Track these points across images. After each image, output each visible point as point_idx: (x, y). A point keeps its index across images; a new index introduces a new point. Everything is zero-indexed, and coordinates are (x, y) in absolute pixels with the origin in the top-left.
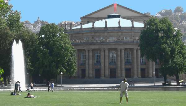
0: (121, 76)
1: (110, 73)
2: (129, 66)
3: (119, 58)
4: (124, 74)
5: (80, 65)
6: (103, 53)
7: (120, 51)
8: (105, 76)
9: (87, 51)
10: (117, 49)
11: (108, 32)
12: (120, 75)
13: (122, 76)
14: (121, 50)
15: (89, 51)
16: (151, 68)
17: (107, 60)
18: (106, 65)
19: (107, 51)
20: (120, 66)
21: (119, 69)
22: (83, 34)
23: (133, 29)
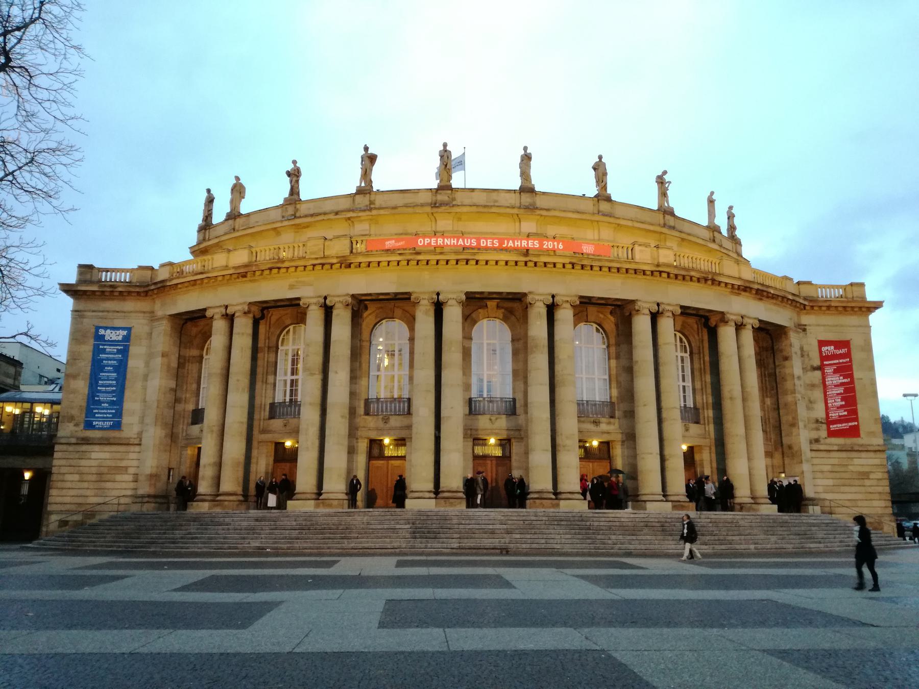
0: (556, 493)
2: (604, 427)
3: (539, 361)
7: (544, 311)
8: (437, 490)
12: (549, 487)
13: (562, 487)
14: (551, 309)
16: (742, 446)
17: (451, 376)
19: (453, 315)
21: (540, 439)
23: (604, 206)
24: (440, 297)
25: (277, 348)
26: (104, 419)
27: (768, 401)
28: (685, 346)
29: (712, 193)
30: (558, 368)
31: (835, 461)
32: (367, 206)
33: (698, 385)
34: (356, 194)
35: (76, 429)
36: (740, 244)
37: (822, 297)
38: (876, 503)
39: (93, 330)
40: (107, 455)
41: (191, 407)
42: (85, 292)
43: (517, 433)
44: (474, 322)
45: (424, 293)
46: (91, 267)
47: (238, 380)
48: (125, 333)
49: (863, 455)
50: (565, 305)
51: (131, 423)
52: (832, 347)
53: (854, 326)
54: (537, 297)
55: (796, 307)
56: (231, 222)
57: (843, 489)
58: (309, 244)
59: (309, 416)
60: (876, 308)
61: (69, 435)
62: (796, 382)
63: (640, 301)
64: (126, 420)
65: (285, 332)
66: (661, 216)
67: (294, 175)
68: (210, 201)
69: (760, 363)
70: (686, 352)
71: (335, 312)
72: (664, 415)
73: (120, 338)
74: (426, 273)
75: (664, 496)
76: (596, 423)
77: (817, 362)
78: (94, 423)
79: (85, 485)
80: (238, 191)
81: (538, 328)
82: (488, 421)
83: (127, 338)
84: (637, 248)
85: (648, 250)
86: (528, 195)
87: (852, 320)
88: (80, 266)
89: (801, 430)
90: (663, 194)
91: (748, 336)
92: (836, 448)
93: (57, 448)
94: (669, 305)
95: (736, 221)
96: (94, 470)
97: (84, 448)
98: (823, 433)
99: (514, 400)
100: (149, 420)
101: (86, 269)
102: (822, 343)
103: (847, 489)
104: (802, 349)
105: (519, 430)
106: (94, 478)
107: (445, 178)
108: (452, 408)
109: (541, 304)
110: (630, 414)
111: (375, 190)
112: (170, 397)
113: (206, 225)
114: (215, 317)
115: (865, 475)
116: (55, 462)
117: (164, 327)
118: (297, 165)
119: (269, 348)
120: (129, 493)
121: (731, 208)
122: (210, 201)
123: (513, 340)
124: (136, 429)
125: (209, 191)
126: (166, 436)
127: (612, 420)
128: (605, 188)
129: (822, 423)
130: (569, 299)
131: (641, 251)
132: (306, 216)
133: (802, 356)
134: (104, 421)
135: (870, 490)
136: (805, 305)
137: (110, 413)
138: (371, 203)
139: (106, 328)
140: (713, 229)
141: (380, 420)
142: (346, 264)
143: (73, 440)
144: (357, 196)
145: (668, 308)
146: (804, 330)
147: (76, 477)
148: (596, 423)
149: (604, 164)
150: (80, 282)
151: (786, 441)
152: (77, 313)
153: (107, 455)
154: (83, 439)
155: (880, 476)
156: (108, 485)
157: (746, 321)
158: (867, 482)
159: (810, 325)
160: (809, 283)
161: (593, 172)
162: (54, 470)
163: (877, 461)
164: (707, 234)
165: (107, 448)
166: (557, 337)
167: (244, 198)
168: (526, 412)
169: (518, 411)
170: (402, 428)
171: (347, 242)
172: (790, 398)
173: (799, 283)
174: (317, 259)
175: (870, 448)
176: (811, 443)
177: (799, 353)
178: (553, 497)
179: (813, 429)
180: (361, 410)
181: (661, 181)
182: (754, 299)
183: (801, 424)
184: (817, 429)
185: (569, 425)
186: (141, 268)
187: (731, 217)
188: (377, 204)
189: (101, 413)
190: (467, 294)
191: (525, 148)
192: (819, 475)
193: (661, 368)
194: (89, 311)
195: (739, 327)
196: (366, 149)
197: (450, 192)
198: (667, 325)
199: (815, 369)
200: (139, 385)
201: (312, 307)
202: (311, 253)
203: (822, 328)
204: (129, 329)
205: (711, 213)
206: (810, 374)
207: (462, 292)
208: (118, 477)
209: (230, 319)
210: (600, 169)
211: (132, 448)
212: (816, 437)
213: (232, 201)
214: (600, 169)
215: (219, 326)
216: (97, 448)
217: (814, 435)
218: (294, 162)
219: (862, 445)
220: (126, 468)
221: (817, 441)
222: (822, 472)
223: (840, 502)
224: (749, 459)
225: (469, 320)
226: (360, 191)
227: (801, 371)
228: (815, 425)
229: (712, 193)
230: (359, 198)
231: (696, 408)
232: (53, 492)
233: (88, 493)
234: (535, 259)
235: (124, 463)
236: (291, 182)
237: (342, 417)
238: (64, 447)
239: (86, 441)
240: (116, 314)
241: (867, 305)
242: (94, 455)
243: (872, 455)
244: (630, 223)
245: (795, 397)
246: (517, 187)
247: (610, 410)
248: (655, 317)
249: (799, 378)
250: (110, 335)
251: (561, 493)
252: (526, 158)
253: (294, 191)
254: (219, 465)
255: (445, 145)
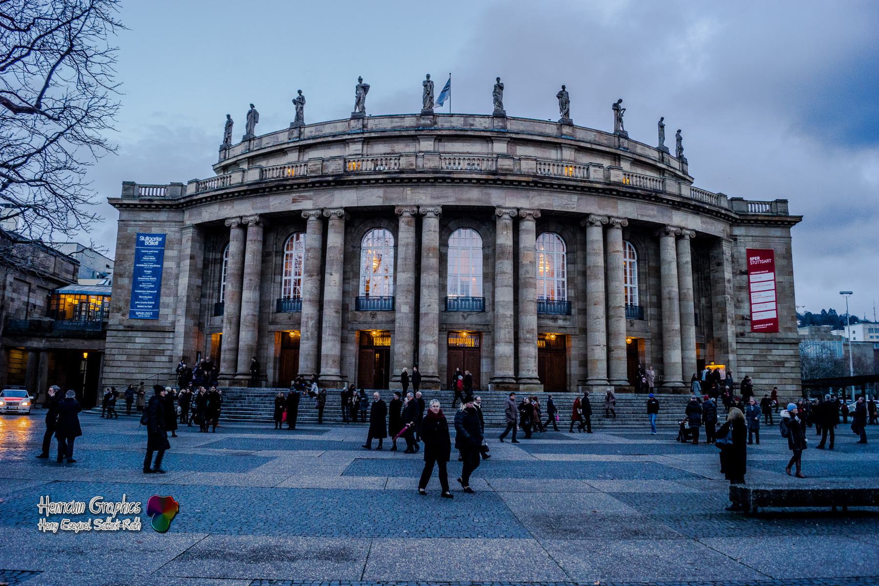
1: (445, 362)
2: (560, 322)
3: (506, 266)
4: (531, 367)
5: (273, 308)
6: (406, 234)
7: (509, 222)
9: (313, 224)
10: (493, 209)
11: (439, 138)
12: (511, 373)
13: (523, 373)
15: (324, 221)
16: (678, 339)
17: (429, 278)
18: (423, 310)
19: (432, 224)
20: (510, 312)
21: (505, 332)
22: (303, 149)
23: (566, 130)
24: (421, 210)
25: (283, 253)
26: (145, 310)
27: (703, 301)
28: (633, 253)
29: (662, 119)
30: (522, 272)
31: (757, 352)
32: (360, 129)
33: (644, 287)
34: (352, 119)
35: (124, 318)
36: (687, 164)
37: (752, 211)
38: (789, 387)
39: (135, 237)
40: (148, 340)
41: (215, 301)
42: (128, 205)
43: (486, 328)
44: (451, 232)
45: (406, 206)
46: (133, 184)
47: (251, 280)
48: (161, 239)
49: (781, 347)
50: (528, 217)
51: (167, 315)
52: (758, 258)
53: (777, 237)
54: (504, 211)
55: (728, 220)
56: (247, 143)
57: (762, 375)
58: (309, 164)
59: (308, 310)
60: (796, 222)
61: (117, 323)
62: (727, 284)
63: (593, 214)
64: (162, 311)
65: (290, 238)
66: (616, 139)
67: (300, 102)
68: (229, 124)
69: (696, 269)
70: (634, 258)
71: (330, 223)
72: (612, 313)
73: (157, 243)
74: (408, 189)
75: (609, 381)
76: (555, 319)
77: (744, 268)
78: (137, 313)
79: (131, 364)
80: (253, 116)
81: (505, 238)
82: (461, 317)
83: (162, 244)
84: (592, 169)
85: (601, 170)
86: (500, 120)
87: (776, 232)
88: (124, 183)
89: (729, 326)
90: (619, 119)
91: (686, 246)
92: (758, 341)
93: (109, 333)
94: (618, 218)
95: (684, 143)
96: (138, 352)
97: (130, 334)
98: (748, 329)
99: (484, 299)
100: (181, 311)
101: (128, 186)
102: (751, 253)
103: (765, 375)
104: (732, 256)
105: (488, 325)
106: (138, 358)
107: (428, 105)
108: (429, 305)
109: (507, 216)
110: (584, 312)
111: (367, 115)
112: (197, 292)
113: (226, 147)
114: (233, 226)
115: (780, 364)
116: (107, 345)
117: (189, 234)
118: (302, 94)
119: (276, 252)
120: (166, 371)
121: (679, 131)
122: (229, 124)
123: (483, 248)
124: (170, 319)
125: (228, 116)
126: (195, 325)
127: (568, 317)
128: (567, 114)
129: (747, 319)
130: (531, 212)
131: (595, 171)
132: (309, 139)
133: (733, 262)
134: (145, 312)
135: (784, 376)
136: (736, 219)
137: (150, 305)
138: (364, 126)
139: (145, 235)
140: (662, 150)
141: (369, 315)
142: (340, 182)
143: (121, 328)
144: (352, 121)
145: (617, 220)
146: (735, 240)
147: (125, 358)
148: (555, 319)
149: (567, 93)
150: (125, 196)
151: (716, 334)
152: (121, 222)
153: (148, 340)
154: (128, 327)
155: (793, 364)
156: (150, 364)
157: (684, 231)
158: (782, 370)
159: (740, 236)
160: (741, 200)
161: (558, 100)
162: (107, 351)
163: (791, 352)
164: (655, 155)
165: (148, 334)
166: (522, 245)
167: (257, 122)
168: (493, 310)
169: (487, 309)
170: (387, 322)
171: (341, 162)
172: (719, 298)
173: (733, 200)
174: (315, 177)
175: (786, 341)
176: (737, 336)
177: (730, 259)
178: (514, 381)
179: (739, 325)
180: (352, 307)
181: (617, 107)
182: (692, 213)
183: (729, 320)
184: (743, 325)
185: (530, 320)
186: (173, 185)
187: (679, 139)
188: (369, 127)
189: (142, 305)
190: (443, 207)
191: (498, 79)
192: (743, 363)
193: (609, 273)
194: (132, 221)
195: (679, 237)
196: (360, 80)
197: (432, 117)
198: (617, 235)
199: (742, 273)
200: (172, 283)
201: (312, 218)
202: (312, 172)
203: (750, 238)
204: (164, 236)
205: (662, 137)
206: (738, 278)
207: (439, 205)
208: (157, 358)
209: (243, 227)
210: (563, 98)
211: (167, 335)
212: (742, 331)
213: (247, 126)
214: (563, 98)
215: (235, 233)
216: (140, 334)
217: (740, 330)
218: (300, 92)
219: (780, 339)
220: (164, 350)
221: (742, 334)
222: (745, 361)
223: (760, 387)
224: (682, 350)
225: (445, 230)
226: (355, 117)
227: (731, 275)
228: (740, 322)
229: (662, 119)
230: (353, 123)
231: (641, 308)
232: (106, 369)
233: (133, 370)
234: (502, 178)
235: (161, 347)
236: (297, 109)
237: (337, 312)
238: (115, 333)
239: (131, 328)
240: (154, 223)
241: (789, 219)
242: (137, 340)
243: (788, 346)
244: (589, 146)
245: (725, 298)
246: (491, 113)
247: (567, 309)
248: (607, 228)
249: (729, 281)
250: (150, 241)
251: (521, 379)
252: (499, 88)
253: (299, 117)
254: (236, 350)
255: (428, 76)
